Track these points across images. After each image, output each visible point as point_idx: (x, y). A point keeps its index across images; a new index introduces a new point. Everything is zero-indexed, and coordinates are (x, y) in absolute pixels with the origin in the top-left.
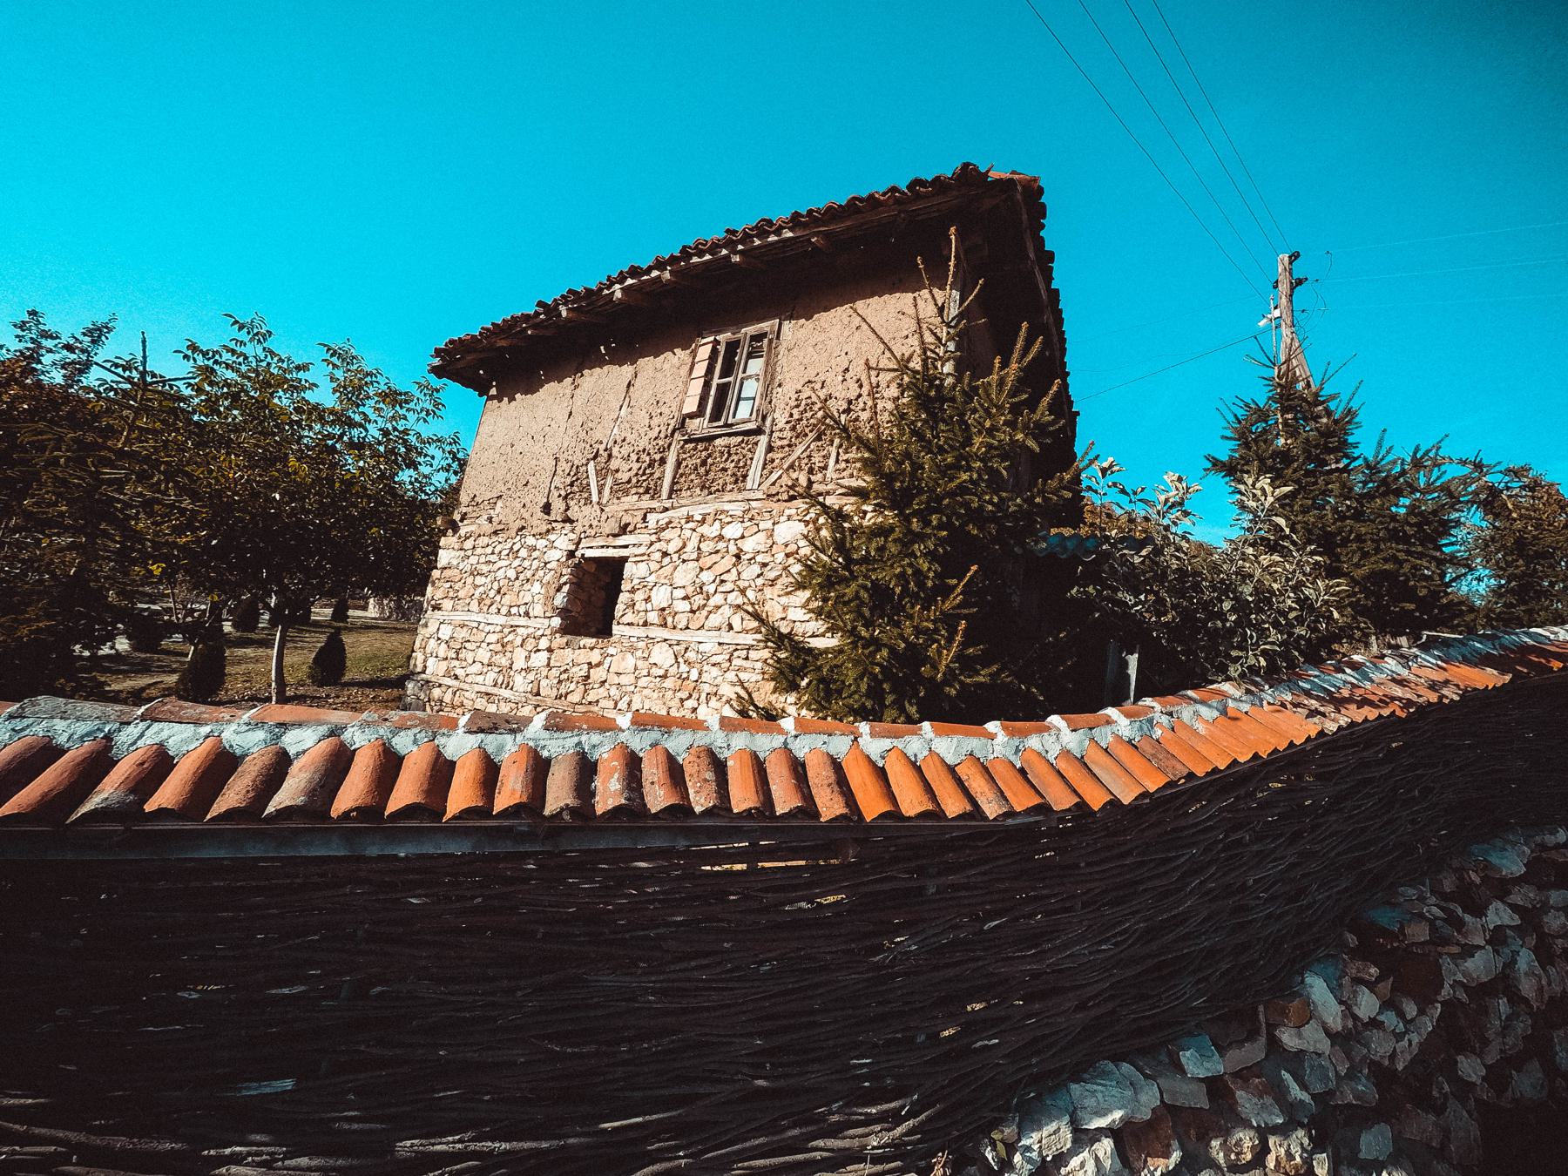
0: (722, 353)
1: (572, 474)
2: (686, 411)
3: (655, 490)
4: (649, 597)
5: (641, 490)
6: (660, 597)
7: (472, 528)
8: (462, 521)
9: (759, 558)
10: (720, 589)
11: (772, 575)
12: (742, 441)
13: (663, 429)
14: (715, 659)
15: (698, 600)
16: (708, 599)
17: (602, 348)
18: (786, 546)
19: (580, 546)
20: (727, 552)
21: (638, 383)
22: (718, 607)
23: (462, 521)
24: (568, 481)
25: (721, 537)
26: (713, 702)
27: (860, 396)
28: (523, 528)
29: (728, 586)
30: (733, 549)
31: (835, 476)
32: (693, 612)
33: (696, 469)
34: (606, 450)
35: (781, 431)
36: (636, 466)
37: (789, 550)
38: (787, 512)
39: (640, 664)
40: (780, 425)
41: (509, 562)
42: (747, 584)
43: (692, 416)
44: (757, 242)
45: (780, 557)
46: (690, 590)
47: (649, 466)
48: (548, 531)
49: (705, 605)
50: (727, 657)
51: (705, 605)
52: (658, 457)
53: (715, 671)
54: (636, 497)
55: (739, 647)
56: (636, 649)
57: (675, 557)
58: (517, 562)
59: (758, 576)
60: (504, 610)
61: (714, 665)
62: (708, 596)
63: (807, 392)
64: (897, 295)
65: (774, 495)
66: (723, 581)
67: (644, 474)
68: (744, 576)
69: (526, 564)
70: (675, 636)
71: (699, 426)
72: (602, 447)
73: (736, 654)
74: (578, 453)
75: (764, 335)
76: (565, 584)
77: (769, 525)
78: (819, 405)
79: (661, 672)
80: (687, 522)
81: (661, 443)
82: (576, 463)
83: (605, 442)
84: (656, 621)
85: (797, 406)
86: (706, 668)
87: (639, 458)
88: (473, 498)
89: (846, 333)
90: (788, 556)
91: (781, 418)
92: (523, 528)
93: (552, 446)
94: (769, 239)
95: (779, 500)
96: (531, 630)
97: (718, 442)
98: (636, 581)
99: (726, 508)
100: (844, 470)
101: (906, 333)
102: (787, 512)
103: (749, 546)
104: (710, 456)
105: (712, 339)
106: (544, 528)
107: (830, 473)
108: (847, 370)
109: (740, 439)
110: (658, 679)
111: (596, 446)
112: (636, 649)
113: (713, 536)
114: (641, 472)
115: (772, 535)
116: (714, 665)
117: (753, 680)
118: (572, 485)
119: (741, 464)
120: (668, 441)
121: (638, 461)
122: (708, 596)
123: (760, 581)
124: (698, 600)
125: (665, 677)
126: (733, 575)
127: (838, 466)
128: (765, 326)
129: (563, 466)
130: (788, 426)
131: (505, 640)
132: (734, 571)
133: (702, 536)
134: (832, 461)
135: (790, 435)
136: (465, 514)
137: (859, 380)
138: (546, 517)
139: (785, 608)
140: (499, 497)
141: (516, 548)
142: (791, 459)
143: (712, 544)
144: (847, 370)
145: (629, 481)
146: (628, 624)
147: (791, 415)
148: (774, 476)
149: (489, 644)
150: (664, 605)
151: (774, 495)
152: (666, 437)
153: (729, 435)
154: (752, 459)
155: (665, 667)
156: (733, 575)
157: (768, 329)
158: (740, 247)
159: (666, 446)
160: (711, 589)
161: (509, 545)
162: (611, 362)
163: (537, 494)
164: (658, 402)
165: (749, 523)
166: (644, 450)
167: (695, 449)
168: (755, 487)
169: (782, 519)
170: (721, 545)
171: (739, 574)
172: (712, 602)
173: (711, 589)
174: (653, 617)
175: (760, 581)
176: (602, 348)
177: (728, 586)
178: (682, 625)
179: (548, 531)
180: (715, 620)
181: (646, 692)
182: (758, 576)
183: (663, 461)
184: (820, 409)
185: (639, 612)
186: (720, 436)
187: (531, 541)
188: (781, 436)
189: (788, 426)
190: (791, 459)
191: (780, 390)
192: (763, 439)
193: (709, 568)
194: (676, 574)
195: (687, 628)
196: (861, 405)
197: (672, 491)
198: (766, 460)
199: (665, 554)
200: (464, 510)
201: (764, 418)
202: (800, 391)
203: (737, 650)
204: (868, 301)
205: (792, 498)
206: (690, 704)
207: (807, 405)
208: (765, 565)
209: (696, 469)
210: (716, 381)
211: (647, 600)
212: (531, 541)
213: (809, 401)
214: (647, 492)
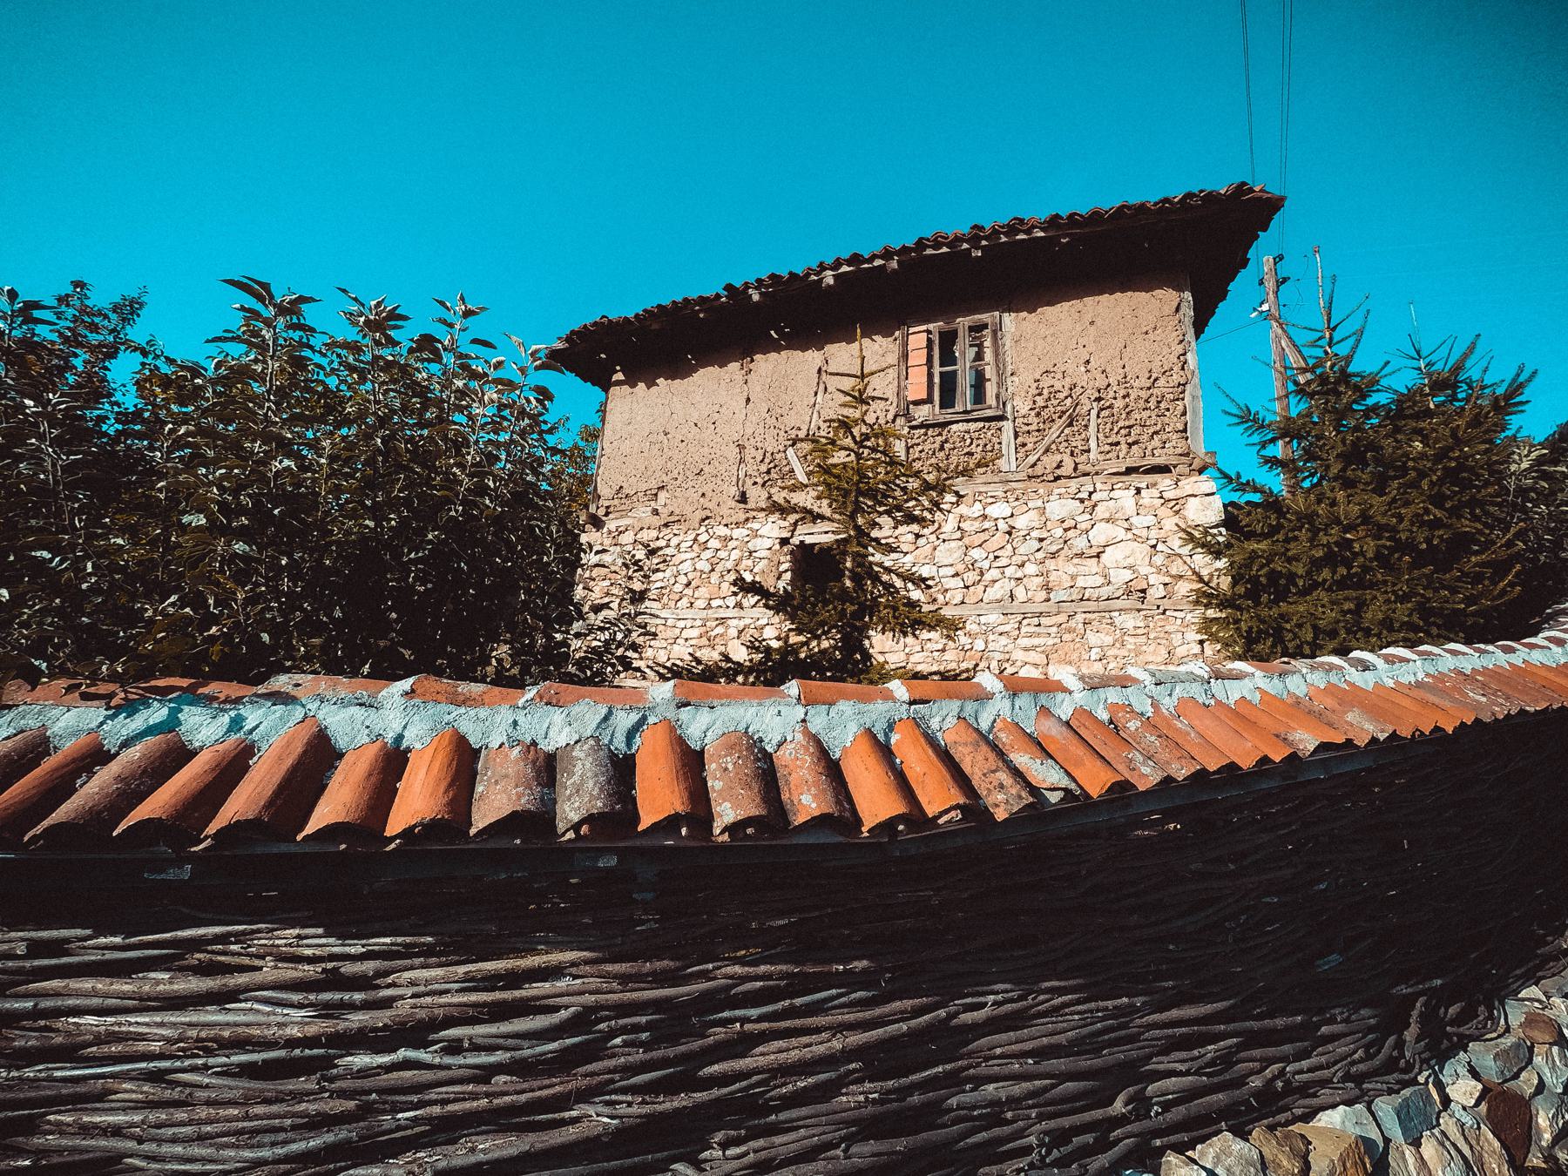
0: (937, 342)
1: (767, 461)
2: (912, 396)
7: (623, 522)
8: (607, 514)
9: (1035, 534)
11: (1054, 548)
12: (984, 427)
14: (1001, 629)
15: (971, 577)
16: (982, 574)
17: (772, 332)
18: (1063, 522)
19: (796, 533)
20: (997, 530)
22: (995, 581)
23: (607, 514)
24: (764, 468)
25: (985, 517)
28: (707, 518)
29: (1003, 562)
30: (1002, 526)
31: (1101, 457)
32: (967, 587)
33: (934, 453)
37: (1066, 525)
38: (1057, 491)
40: (1023, 412)
41: (695, 555)
42: (1026, 558)
43: (917, 403)
44: (1004, 239)
45: (1059, 532)
46: (960, 567)
48: (747, 520)
49: (980, 581)
50: (1016, 626)
51: (980, 581)
53: (1004, 640)
55: (1029, 615)
58: (707, 554)
59: (1038, 550)
60: (701, 603)
61: (1001, 634)
62: (981, 572)
63: (1046, 382)
66: (996, 557)
68: (1022, 550)
69: (722, 554)
71: (922, 413)
73: (1025, 622)
74: (769, 439)
75: (985, 326)
76: (786, 571)
77: (1039, 503)
78: (1065, 394)
82: (770, 449)
85: (1040, 394)
86: (991, 637)
88: (618, 492)
90: (1066, 530)
91: (1023, 406)
92: (707, 518)
93: (732, 432)
94: (1018, 237)
95: (1044, 481)
96: (748, 621)
97: (954, 427)
99: (981, 490)
102: (1057, 491)
103: (1021, 523)
104: (946, 441)
105: (924, 327)
106: (742, 516)
107: (1092, 455)
108: (1088, 362)
109: (981, 424)
110: (936, 654)
113: (976, 515)
116: (1001, 634)
118: (768, 472)
119: (989, 448)
122: (981, 572)
123: (1040, 555)
124: (971, 577)
127: (1102, 449)
128: (985, 317)
129: (750, 452)
130: (1033, 413)
133: (961, 517)
135: (1036, 420)
136: (608, 507)
137: (1103, 372)
138: (742, 506)
139: (1073, 577)
140: (661, 488)
141: (702, 538)
142: (1047, 441)
144: (1088, 362)
147: (1034, 402)
148: (1032, 459)
152: (887, 422)
154: (1000, 443)
157: (989, 321)
158: (984, 243)
160: (986, 564)
161: (693, 537)
162: (786, 348)
163: (720, 482)
165: (1017, 503)
167: (926, 434)
168: (1013, 468)
169: (1051, 498)
170: (987, 525)
172: (988, 577)
173: (986, 564)
175: (1040, 555)
176: (772, 332)
177: (1003, 562)
178: (958, 600)
179: (747, 520)
180: (995, 592)
182: (1038, 550)
184: (1066, 397)
186: (957, 422)
187: (722, 531)
188: (1026, 421)
189: (1033, 413)
190: (1047, 441)
191: (1015, 378)
192: (1007, 426)
193: (980, 545)
195: (963, 603)
200: (607, 503)
201: (1004, 404)
202: (1038, 381)
205: (1057, 478)
207: (1051, 393)
208: (1041, 540)
212: (722, 531)
213: (1052, 390)
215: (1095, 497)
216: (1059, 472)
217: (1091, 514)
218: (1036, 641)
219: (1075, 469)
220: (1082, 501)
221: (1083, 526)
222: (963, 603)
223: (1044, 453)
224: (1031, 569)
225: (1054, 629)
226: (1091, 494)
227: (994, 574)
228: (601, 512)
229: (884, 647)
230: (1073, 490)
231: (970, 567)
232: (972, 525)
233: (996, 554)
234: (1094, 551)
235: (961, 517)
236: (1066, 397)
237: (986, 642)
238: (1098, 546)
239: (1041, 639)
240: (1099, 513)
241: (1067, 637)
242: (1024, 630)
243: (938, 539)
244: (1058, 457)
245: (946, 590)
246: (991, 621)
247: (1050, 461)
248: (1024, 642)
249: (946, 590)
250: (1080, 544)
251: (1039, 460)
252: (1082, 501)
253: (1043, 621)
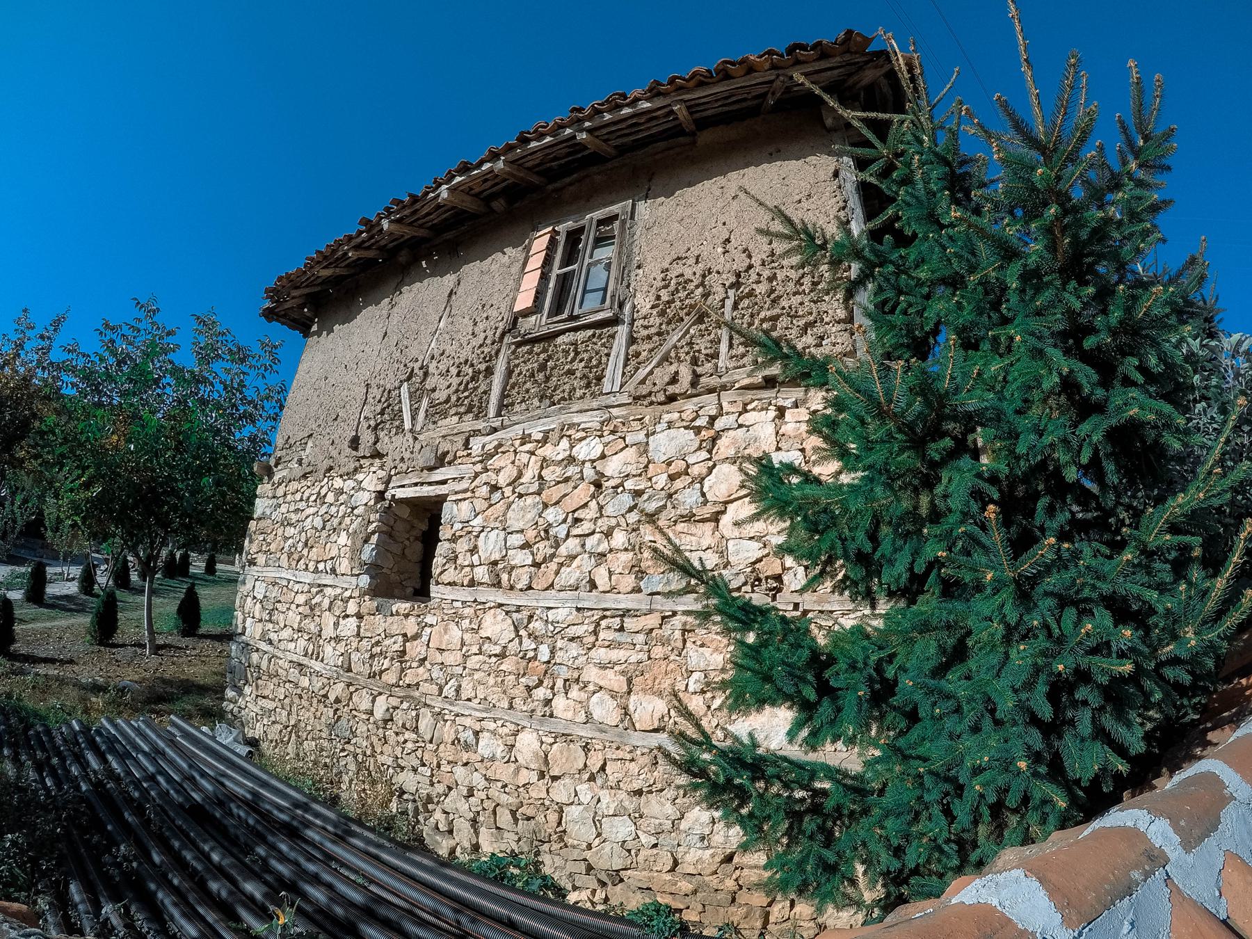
0: (562, 243)
1: (383, 400)
2: (518, 307)
3: (480, 407)
4: (476, 547)
5: (462, 409)
6: (490, 546)
7: (284, 473)
8: (276, 466)
9: (629, 484)
10: (575, 531)
11: (651, 507)
12: (594, 335)
13: (490, 333)
14: (572, 631)
15: (543, 549)
17: (424, 263)
18: (669, 464)
19: (391, 485)
20: (582, 479)
21: (460, 291)
22: (573, 557)
24: (379, 409)
25: (571, 460)
26: (575, 693)
27: (750, 267)
28: (331, 468)
29: (585, 527)
30: (589, 472)
31: (731, 364)
32: (536, 565)
33: (532, 375)
34: (421, 368)
35: (645, 318)
36: (455, 381)
37: (673, 469)
38: (666, 417)
39: (467, 637)
40: (644, 311)
41: (316, 509)
42: (613, 522)
43: (526, 313)
45: (662, 480)
46: (531, 534)
47: (473, 379)
48: (356, 470)
49: (553, 556)
50: (591, 628)
51: (553, 556)
52: (483, 367)
53: (574, 650)
54: (456, 418)
55: (608, 613)
56: (462, 618)
57: (508, 491)
58: (323, 509)
59: (631, 510)
60: (311, 566)
61: (572, 639)
63: (677, 269)
64: (778, 163)
65: (645, 397)
67: (466, 389)
68: (609, 510)
69: (333, 509)
70: (514, 600)
72: (418, 365)
73: (604, 623)
74: (391, 375)
75: (616, 217)
76: (373, 533)
77: (641, 437)
78: (696, 282)
79: (497, 650)
80: (522, 444)
81: (486, 350)
82: (388, 386)
83: (421, 358)
84: (486, 579)
85: (666, 287)
86: (559, 644)
87: (459, 372)
89: (719, 205)
90: (672, 478)
91: (644, 303)
92: (331, 468)
93: (365, 372)
95: (652, 403)
96: (339, 591)
97: (560, 340)
98: (458, 526)
99: (576, 420)
100: (743, 356)
101: (797, 198)
102: (666, 417)
104: (550, 357)
106: (352, 466)
107: (722, 362)
108: (728, 241)
109: (590, 332)
110: (494, 659)
111: (411, 365)
112: (462, 618)
113: (560, 457)
114: (462, 388)
115: (646, 451)
116: (572, 639)
117: (633, 659)
118: (382, 413)
119: (594, 362)
120: (496, 347)
121: (458, 375)
123: (633, 517)
124: (543, 549)
125: (502, 656)
126: (591, 512)
127: (734, 352)
128: (615, 209)
129: (376, 392)
130: (654, 312)
131: (313, 602)
132: (593, 504)
133: (544, 460)
134: (724, 347)
135: (658, 321)
136: (280, 458)
138: (354, 453)
141: (323, 492)
142: (664, 349)
143: (558, 470)
144: (728, 241)
145: (448, 400)
146: (449, 584)
147: (658, 298)
148: (642, 373)
149: (298, 606)
150: (496, 556)
151: (645, 397)
153: (575, 329)
154: (608, 355)
155: (502, 642)
156: (591, 512)
157: (617, 211)
159: (493, 353)
160: (561, 531)
161: (318, 489)
163: (346, 427)
164: (483, 306)
165: (611, 437)
166: (466, 361)
167: (530, 352)
168: (616, 388)
169: (659, 428)
170: (572, 470)
171: (601, 508)
172: (563, 550)
173: (561, 531)
174: (481, 573)
175: (633, 517)
176: (424, 263)
177: (585, 527)
179: (356, 470)
180: (570, 575)
181: (477, 676)
182: (631, 510)
183: (489, 372)
184: (697, 287)
185: (463, 567)
186: (563, 332)
187: (338, 483)
188: (646, 323)
189: (654, 312)
190: (664, 349)
191: (641, 271)
192: (622, 331)
193: (557, 503)
194: (510, 514)
195: (530, 588)
196: (754, 277)
197: (501, 407)
198: (627, 354)
199: (495, 488)
200: (279, 454)
201: (621, 305)
202: (667, 270)
203: (604, 617)
204: (742, 172)
205: (672, 399)
206: (541, 693)
207: (679, 284)
208: (638, 493)
209: (532, 375)
210: (556, 271)
211: (474, 550)
212: (338, 483)
213: (681, 279)
214: (469, 411)
215: (719, 424)
216: (671, 389)
217: (710, 452)
218: (616, 655)
219: (694, 384)
220: (698, 430)
221: (695, 471)
222: (530, 588)
223: (659, 365)
224: (619, 539)
225: (641, 638)
226: (713, 419)
227: (572, 545)
228: (272, 462)
229: (441, 642)
230: (688, 415)
231: (542, 533)
232: (554, 472)
233: (576, 515)
234: (708, 511)
235: (544, 460)
236: (697, 287)
237: (553, 652)
238: (715, 503)
239: (622, 652)
240: (722, 449)
241: (658, 651)
242: (602, 635)
243: (514, 492)
244: (673, 368)
245: (513, 568)
246: (560, 618)
247: (662, 376)
248: (601, 654)
249: (513, 568)
250: (689, 498)
251: (651, 373)
252: (698, 430)
253: (630, 623)
